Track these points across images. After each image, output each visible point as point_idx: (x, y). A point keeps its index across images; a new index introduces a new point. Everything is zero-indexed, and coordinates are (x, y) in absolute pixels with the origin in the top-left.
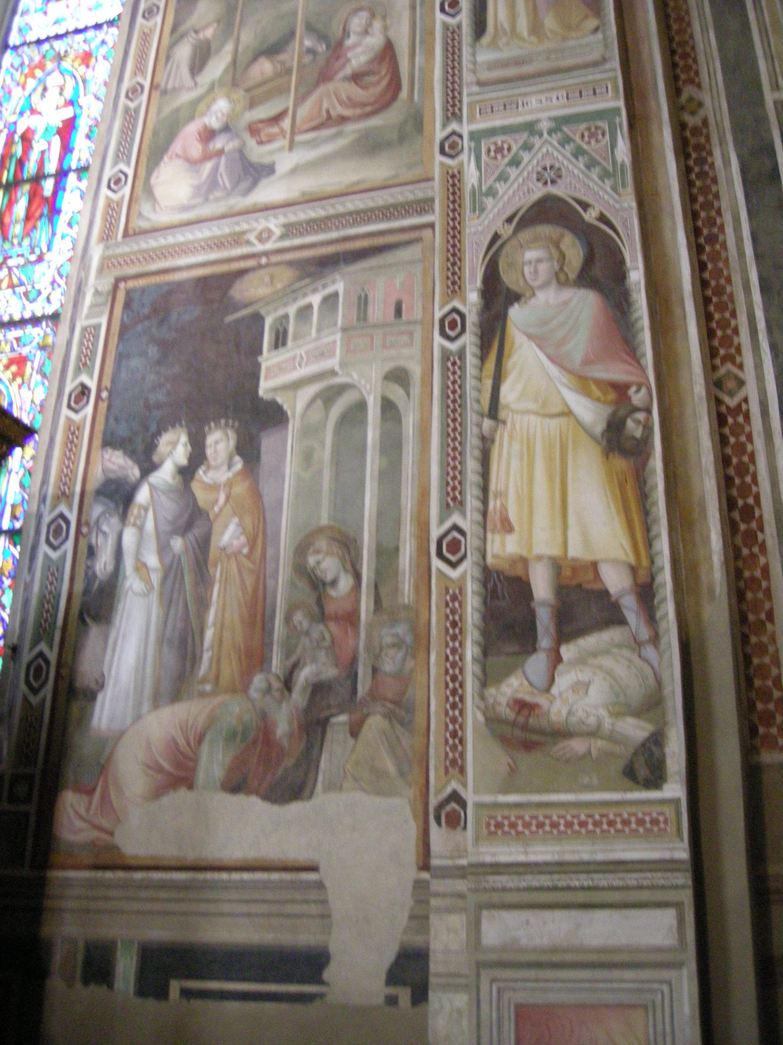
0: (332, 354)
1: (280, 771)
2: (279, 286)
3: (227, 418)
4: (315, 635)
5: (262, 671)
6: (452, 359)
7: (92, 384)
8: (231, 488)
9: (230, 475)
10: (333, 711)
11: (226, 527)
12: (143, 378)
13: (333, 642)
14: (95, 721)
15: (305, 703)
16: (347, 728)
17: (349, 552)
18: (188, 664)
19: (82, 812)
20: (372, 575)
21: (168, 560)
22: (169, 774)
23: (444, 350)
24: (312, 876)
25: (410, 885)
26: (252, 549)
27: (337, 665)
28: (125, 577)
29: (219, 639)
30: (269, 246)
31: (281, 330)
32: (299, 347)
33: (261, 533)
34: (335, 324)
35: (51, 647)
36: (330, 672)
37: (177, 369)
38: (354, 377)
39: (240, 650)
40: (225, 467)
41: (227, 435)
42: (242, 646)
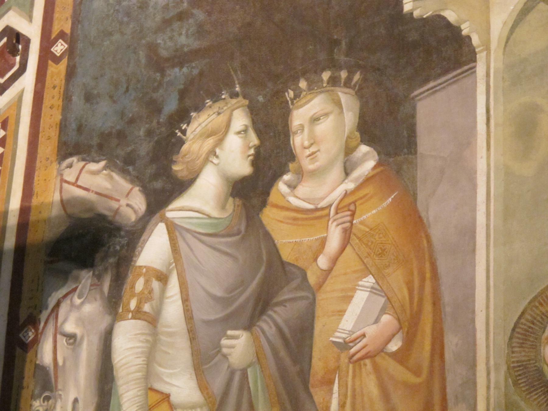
3: (334, 65)
8: (353, 215)
9: (349, 185)
11: (348, 299)
33: (428, 307)
40: (337, 171)
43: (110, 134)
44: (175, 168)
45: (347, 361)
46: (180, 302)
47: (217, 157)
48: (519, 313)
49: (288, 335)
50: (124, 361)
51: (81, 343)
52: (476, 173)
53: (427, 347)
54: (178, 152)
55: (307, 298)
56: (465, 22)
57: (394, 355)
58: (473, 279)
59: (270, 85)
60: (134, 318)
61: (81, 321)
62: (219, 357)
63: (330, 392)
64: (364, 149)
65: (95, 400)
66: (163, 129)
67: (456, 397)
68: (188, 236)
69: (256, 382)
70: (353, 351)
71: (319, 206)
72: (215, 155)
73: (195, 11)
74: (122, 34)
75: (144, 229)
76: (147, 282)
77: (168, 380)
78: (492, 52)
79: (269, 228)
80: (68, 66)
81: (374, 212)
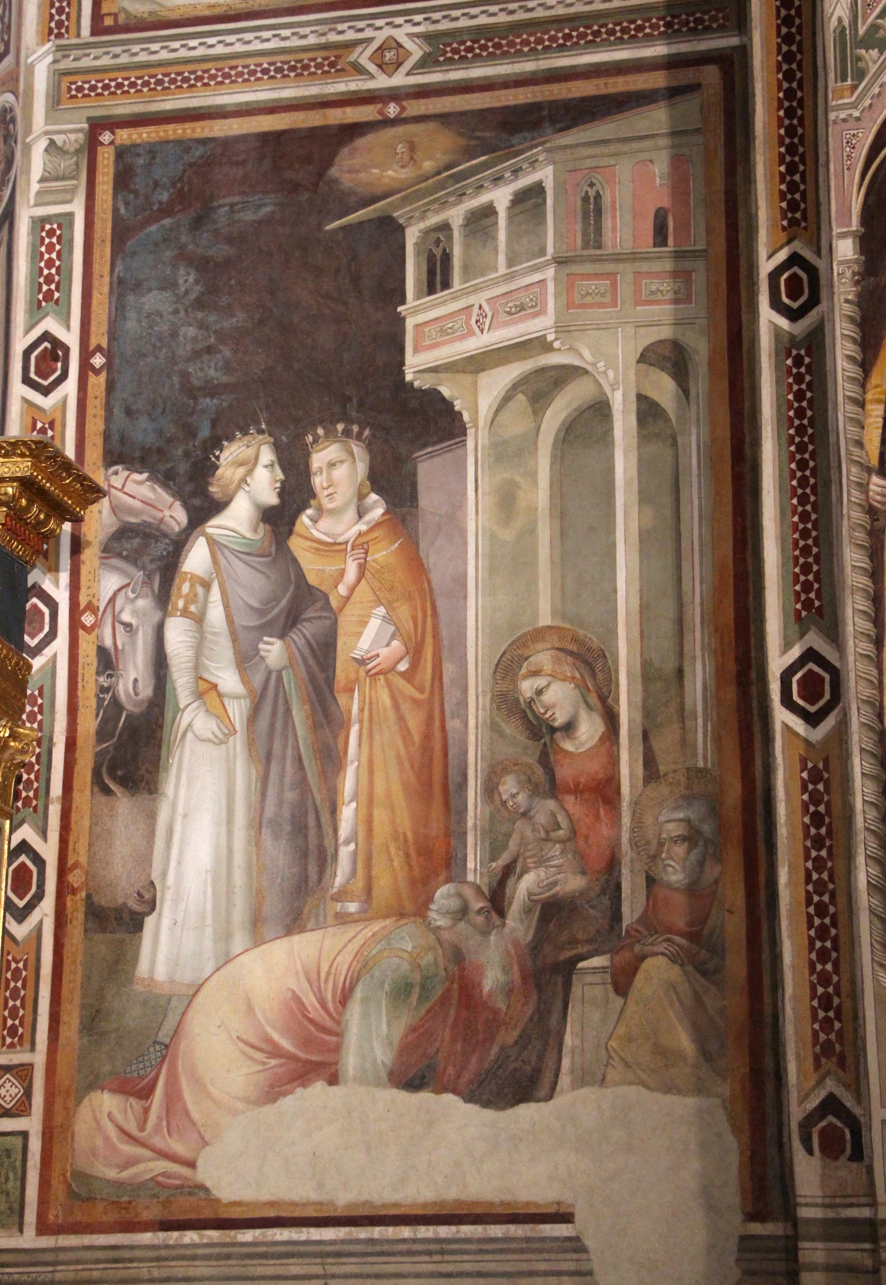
0: (542, 312)
1: (495, 1049)
2: (428, 165)
4: (541, 818)
5: (448, 880)
7: (71, 338)
8: (366, 553)
9: (362, 527)
10: (581, 950)
11: (365, 624)
12: (174, 334)
13: (574, 831)
14: (143, 968)
15: (530, 937)
17: (594, 675)
18: (313, 869)
19: (132, 1128)
20: (638, 717)
21: (258, 680)
24: (561, 1230)
25: (732, 1244)
27: (584, 873)
28: (177, 710)
30: (399, 79)
31: (438, 253)
32: (476, 290)
33: (429, 639)
34: (542, 252)
35: (43, 834)
37: (239, 318)
38: (584, 356)
39: (406, 841)
40: (351, 513)
41: (351, 454)
42: (409, 835)
43: (150, 449)
44: (212, 489)
46: (222, 608)
51: (136, 633)
53: (429, 671)
54: (213, 475)
55: (329, 618)
57: (402, 674)
58: (465, 620)
59: (292, 427)
60: (181, 616)
61: (135, 612)
62: (257, 658)
63: (352, 697)
64: (374, 497)
65: (153, 681)
66: (199, 453)
67: (452, 714)
68: (226, 552)
69: (290, 682)
70: (369, 666)
72: (246, 482)
73: (222, 347)
74: (156, 357)
75: (186, 541)
76: (192, 586)
79: (296, 554)
80: (107, 380)
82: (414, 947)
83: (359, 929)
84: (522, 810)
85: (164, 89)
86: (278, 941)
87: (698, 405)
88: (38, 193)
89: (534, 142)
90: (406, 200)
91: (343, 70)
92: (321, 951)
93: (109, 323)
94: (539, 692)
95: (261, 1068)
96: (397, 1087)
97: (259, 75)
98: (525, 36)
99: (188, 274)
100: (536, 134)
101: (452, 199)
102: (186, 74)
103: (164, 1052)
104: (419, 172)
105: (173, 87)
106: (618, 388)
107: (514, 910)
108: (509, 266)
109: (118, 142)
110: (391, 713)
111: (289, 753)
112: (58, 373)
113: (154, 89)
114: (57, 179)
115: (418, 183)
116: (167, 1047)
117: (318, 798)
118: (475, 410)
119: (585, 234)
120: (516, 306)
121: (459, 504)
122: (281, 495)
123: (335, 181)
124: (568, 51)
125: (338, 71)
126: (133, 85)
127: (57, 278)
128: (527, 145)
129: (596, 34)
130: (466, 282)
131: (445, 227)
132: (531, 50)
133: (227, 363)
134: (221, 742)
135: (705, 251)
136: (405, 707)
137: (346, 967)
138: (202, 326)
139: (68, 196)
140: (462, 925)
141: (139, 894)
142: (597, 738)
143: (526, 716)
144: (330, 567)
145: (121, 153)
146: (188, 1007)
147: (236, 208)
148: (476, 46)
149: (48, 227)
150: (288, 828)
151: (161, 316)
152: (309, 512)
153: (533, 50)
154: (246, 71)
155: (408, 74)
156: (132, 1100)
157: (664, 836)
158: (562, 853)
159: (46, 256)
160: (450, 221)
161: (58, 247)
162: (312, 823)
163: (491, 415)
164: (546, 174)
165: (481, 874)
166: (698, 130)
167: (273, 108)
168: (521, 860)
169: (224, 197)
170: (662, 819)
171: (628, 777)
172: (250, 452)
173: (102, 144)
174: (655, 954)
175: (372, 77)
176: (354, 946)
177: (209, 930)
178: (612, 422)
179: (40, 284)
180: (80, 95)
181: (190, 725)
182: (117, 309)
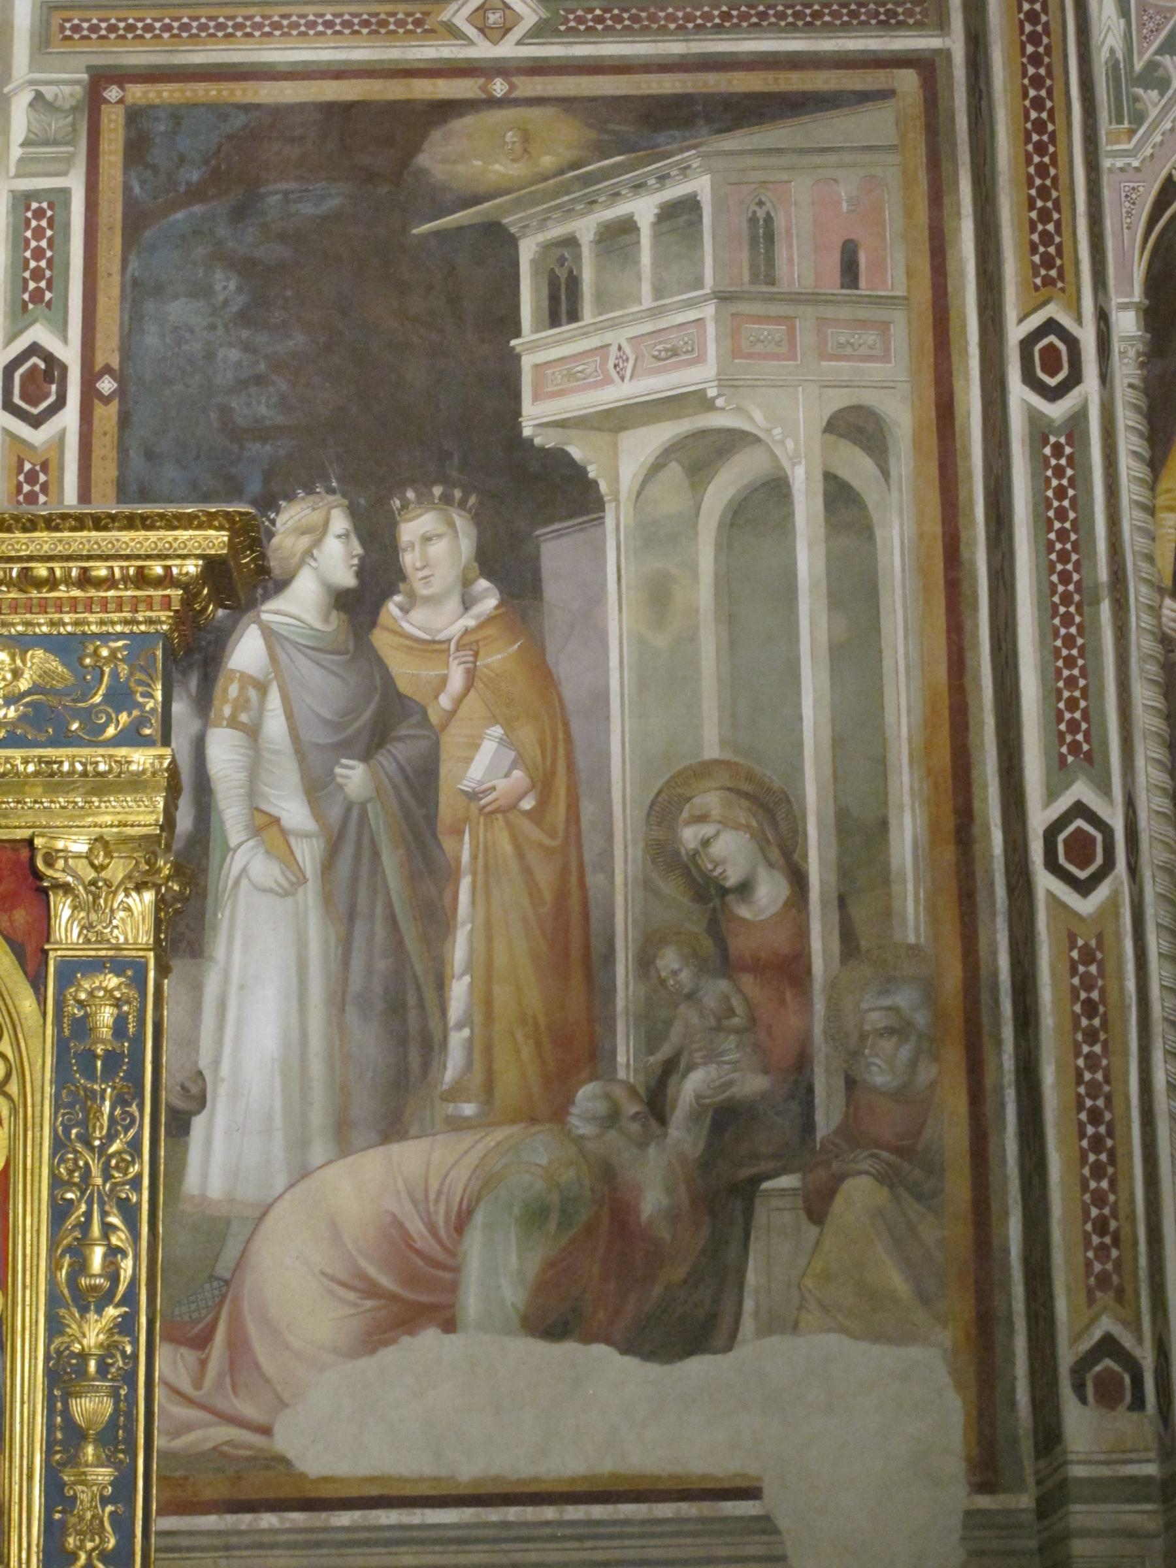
0: (700, 359)
1: (657, 1290)
2: (547, 161)
3: (443, 480)
5: (593, 1077)
6: (1052, 440)
7: (70, 354)
8: (476, 655)
9: (469, 622)
10: (765, 1166)
11: (475, 746)
12: (210, 356)
13: (753, 1020)
14: (192, 1182)
16: (800, 1203)
17: (775, 824)
18: (414, 1059)
19: (185, 1385)
20: (832, 877)
21: (335, 813)
22: (393, 1298)
23: (1034, 418)
25: (956, 1521)
26: (544, 802)
27: (765, 1071)
28: (227, 849)
29: (485, 1001)
30: (507, 49)
31: (562, 274)
32: (614, 325)
33: (561, 769)
34: (699, 283)
36: (753, 1084)
37: (298, 340)
38: (755, 419)
39: (536, 1026)
40: (453, 604)
41: (452, 525)
42: (542, 1020)
45: (477, 812)
46: (283, 718)
47: (315, 560)
48: (656, 790)
49: (411, 774)
50: (221, 774)
52: (607, 634)
55: (429, 737)
56: (592, 463)
57: (527, 814)
60: (229, 726)
62: (332, 787)
63: (462, 840)
64: (483, 583)
68: (288, 645)
70: (483, 802)
71: (438, 638)
72: (312, 556)
73: (274, 377)
76: (242, 688)
77: (275, 802)
78: (622, 505)
80: (120, 412)
81: (499, 656)
82: (551, 1162)
83: (478, 1137)
84: (686, 990)
85: (191, 36)
86: (372, 1151)
87: (901, 489)
88: (21, 160)
89: (687, 143)
90: (518, 204)
91: (432, 31)
92: (428, 1165)
93: (121, 337)
94: (706, 843)
95: (353, 1311)
96: (534, 1336)
97: (320, 28)
98: (670, 10)
99: (228, 279)
100: (687, 134)
101: (579, 207)
102: (221, 20)
103: (224, 1290)
104: (536, 170)
105: (203, 34)
106: (800, 463)
107: (679, 1117)
108: (657, 298)
109: (129, 100)
110: (514, 865)
111: (379, 910)
112: (52, 399)
113: (178, 36)
114: (46, 143)
115: (535, 183)
116: (227, 1283)
117: (418, 967)
118: (615, 480)
119: (753, 266)
120: (666, 350)
121: (596, 598)
122: (360, 573)
123: (423, 172)
124: (727, 33)
125: (426, 31)
126: (148, 28)
127: (48, 273)
128: (675, 146)
129: (763, 16)
130: (600, 314)
131: (571, 242)
132: (679, 27)
133: (283, 397)
134: (286, 894)
135: (906, 298)
136: (532, 857)
137: (461, 1186)
138: (248, 347)
139: (60, 167)
140: (612, 1134)
141: (183, 1087)
142: (780, 903)
143: (689, 873)
144: (429, 672)
145: (134, 115)
146: (253, 1233)
147: (291, 196)
148: (608, 15)
149: (34, 205)
150: (379, 1006)
151: (192, 332)
152: (397, 598)
153: (680, 28)
154: (302, 21)
155: (519, 43)
156: (184, 1350)
157: (867, 1027)
158: (737, 1047)
159: (33, 244)
160: (577, 234)
161: (49, 233)
162: (412, 1000)
163: (636, 487)
164: (701, 185)
165: (636, 1070)
166: (891, 148)
167: (338, 72)
168: (685, 1054)
169: (275, 181)
170: (865, 1006)
171: (820, 953)
172: (316, 517)
173: (107, 102)
174: (859, 1173)
175: (471, 43)
176: (472, 1159)
177: (279, 1137)
178: (792, 504)
179: (25, 281)
180: (76, 36)
181: (244, 870)
182: (131, 318)
